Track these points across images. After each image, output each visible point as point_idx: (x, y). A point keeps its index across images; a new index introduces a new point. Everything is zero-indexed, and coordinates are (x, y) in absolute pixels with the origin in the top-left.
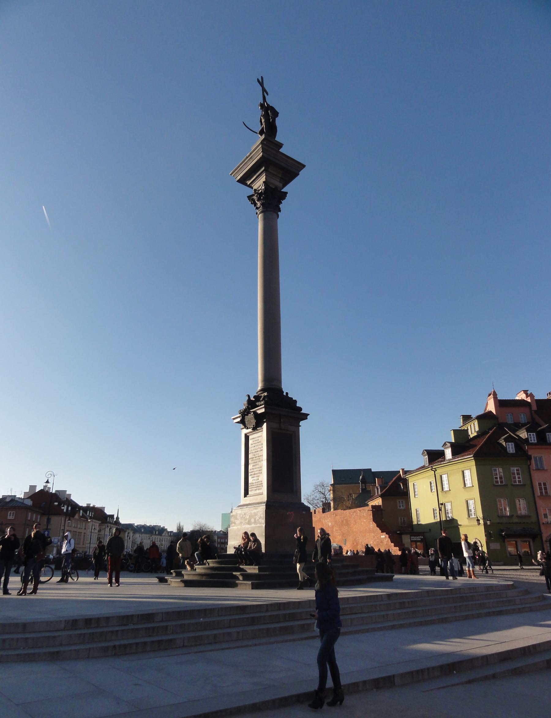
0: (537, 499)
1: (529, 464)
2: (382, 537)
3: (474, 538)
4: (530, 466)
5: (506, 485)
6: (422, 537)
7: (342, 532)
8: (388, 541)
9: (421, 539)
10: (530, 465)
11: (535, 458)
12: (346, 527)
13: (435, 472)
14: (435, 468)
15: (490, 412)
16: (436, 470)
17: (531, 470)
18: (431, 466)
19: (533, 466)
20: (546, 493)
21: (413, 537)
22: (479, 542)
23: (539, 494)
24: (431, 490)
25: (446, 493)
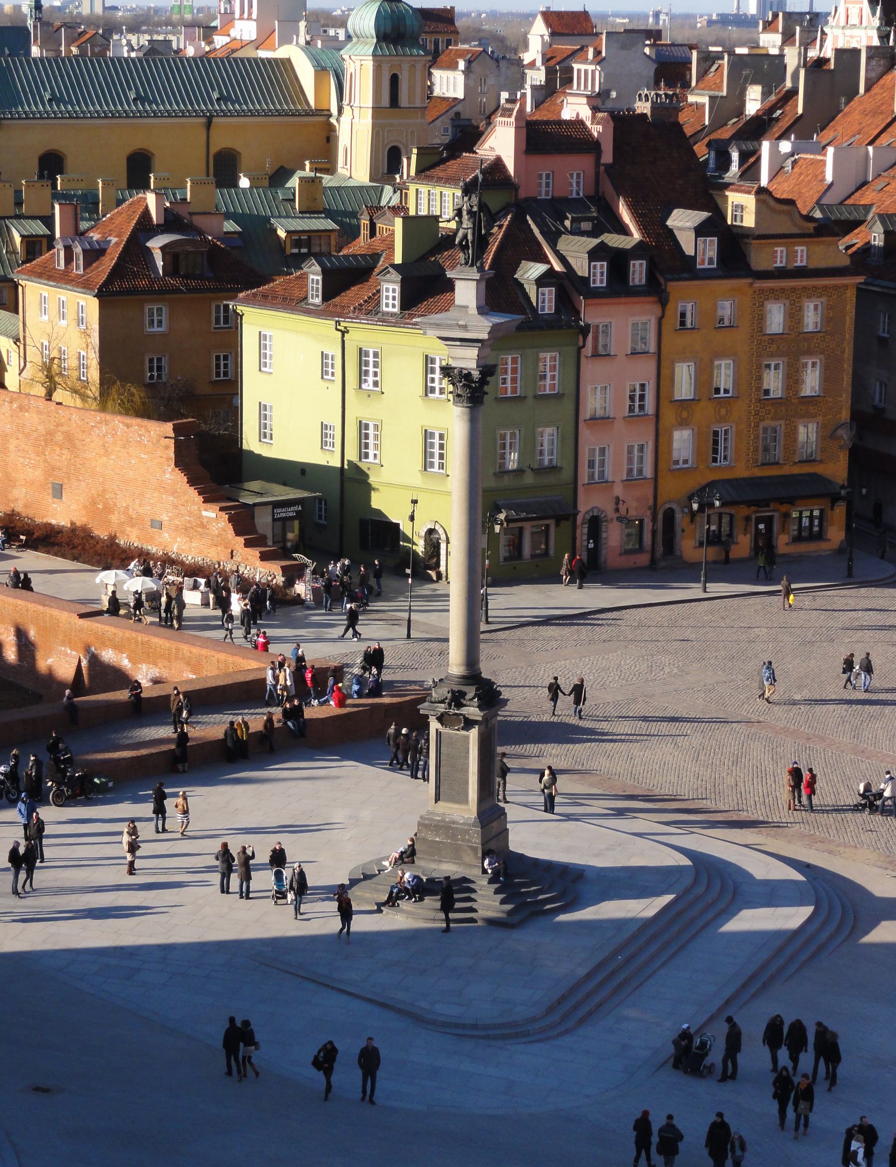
0: (582, 426)
2: (205, 513)
3: (431, 521)
5: (522, 399)
6: (300, 508)
7: (45, 461)
8: (224, 530)
9: (296, 512)
10: (584, 346)
12: (65, 451)
13: (343, 336)
14: (345, 328)
15: (498, 164)
16: (348, 332)
17: (583, 360)
18: (337, 319)
19: (588, 350)
21: (279, 510)
22: (443, 532)
24: (324, 373)
25: (369, 396)
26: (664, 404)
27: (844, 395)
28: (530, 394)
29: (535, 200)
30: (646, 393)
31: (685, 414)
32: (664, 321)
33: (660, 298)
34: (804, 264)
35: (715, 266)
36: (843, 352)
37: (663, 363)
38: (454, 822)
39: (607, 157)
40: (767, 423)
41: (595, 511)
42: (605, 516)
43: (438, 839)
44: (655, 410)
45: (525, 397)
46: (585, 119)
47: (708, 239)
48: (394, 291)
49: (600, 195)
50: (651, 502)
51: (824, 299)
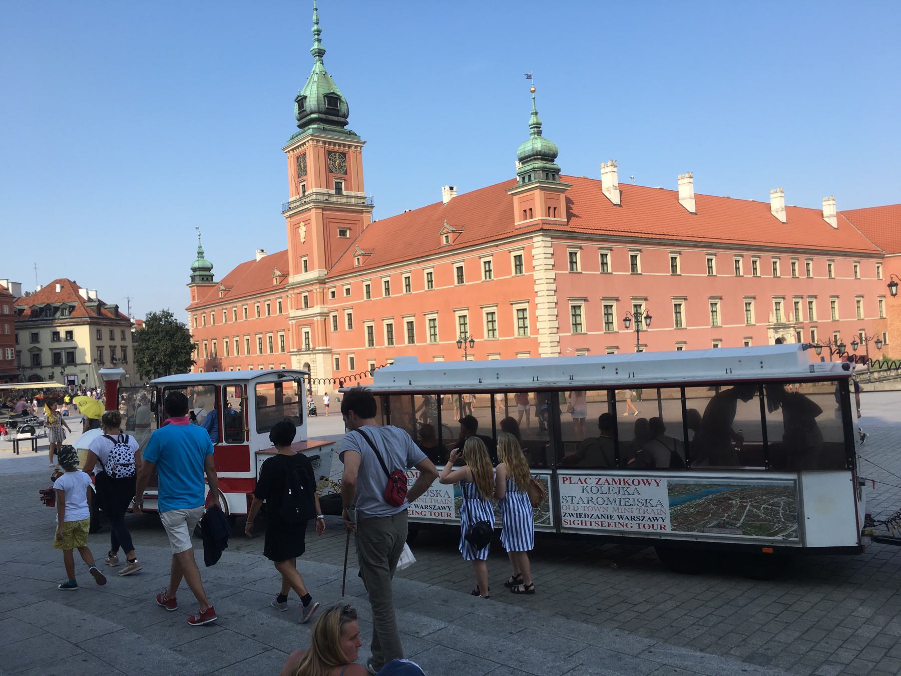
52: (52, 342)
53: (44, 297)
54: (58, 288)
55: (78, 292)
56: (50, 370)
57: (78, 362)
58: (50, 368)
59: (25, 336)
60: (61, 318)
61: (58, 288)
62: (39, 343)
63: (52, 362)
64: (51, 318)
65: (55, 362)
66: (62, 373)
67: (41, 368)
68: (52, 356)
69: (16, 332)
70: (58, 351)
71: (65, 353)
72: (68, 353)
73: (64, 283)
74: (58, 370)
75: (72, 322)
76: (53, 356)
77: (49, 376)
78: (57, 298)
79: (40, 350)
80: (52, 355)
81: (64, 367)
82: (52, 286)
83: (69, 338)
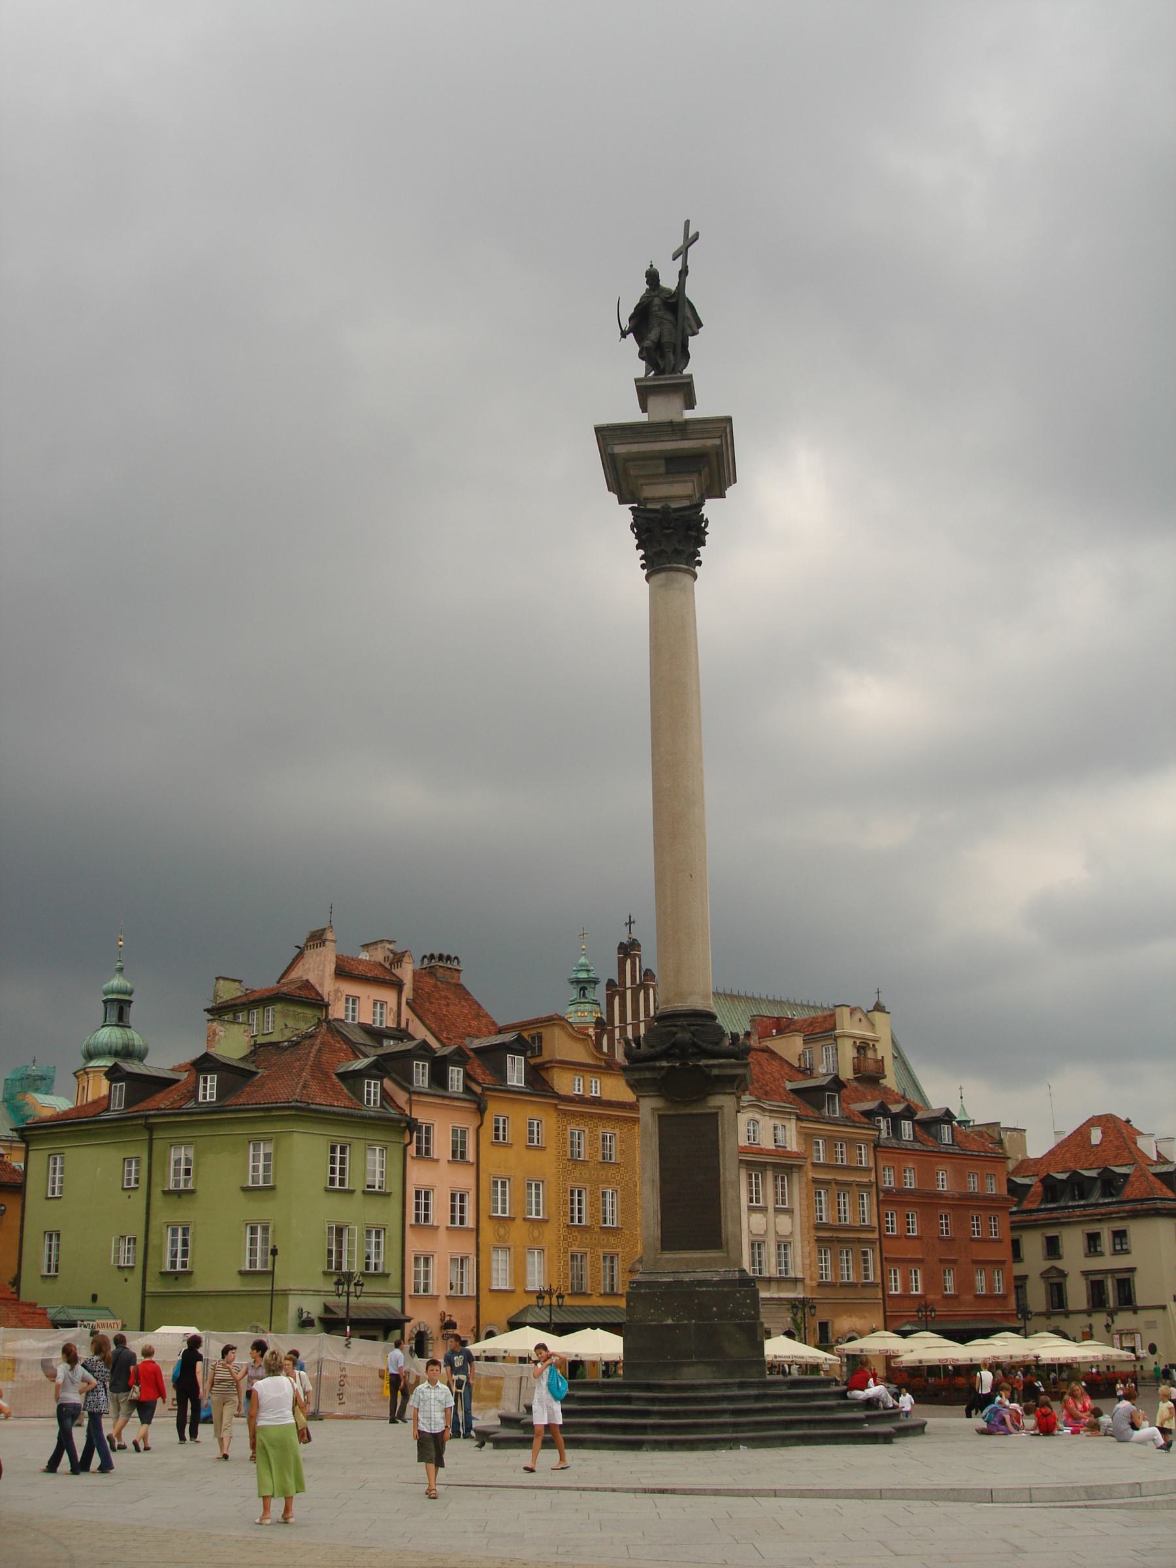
1: (407, 1141)
4: (409, 1147)
11: (419, 1132)
17: (409, 1159)
19: (412, 1150)
20: (427, 1217)
23: (413, 1222)
26: (483, 1219)
27: (638, 1229)
28: (359, 1187)
29: (341, 1020)
30: (466, 1204)
31: (502, 1232)
32: (481, 1130)
33: (479, 1105)
34: (598, 1095)
35: (523, 1085)
36: (636, 1186)
37: (481, 1175)
38: (701, 1283)
39: (407, 992)
40: (574, 1248)
41: (422, 1325)
42: (431, 1333)
43: (670, 1321)
44: (475, 1223)
45: (353, 1192)
46: (383, 963)
47: (516, 1057)
48: (212, 1081)
49: (403, 1025)
50: (474, 1324)
51: (617, 1131)
52: (1086, 1256)
53: (1068, 1155)
54: (1096, 1136)
55: (1136, 1144)
56: (1083, 1320)
57: (1140, 1300)
58: (1083, 1317)
59: (1033, 1244)
60: (1101, 1201)
61: (1096, 1136)
62: (1060, 1257)
63: (1088, 1302)
64: (1082, 1203)
65: (1093, 1303)
66: (1108, 1326)
67: (1067, 1314)
68: (1087, 1287)
69: (1016, 1234)
70: (1098, 1277)
71: (1113, 1281)
72: (1119, 1281)
73: (1106, 1122)
74: (1099, 1319)
75: (1124, 1211)
76: (1090, 1287)
77: (1083, 1333)
78: (1092, 1158)
79: (1063, 1274)
80: (1087, 1284)
81: (1112, 1314)
82: (1082, 1133)
83: (1118, 1247)
